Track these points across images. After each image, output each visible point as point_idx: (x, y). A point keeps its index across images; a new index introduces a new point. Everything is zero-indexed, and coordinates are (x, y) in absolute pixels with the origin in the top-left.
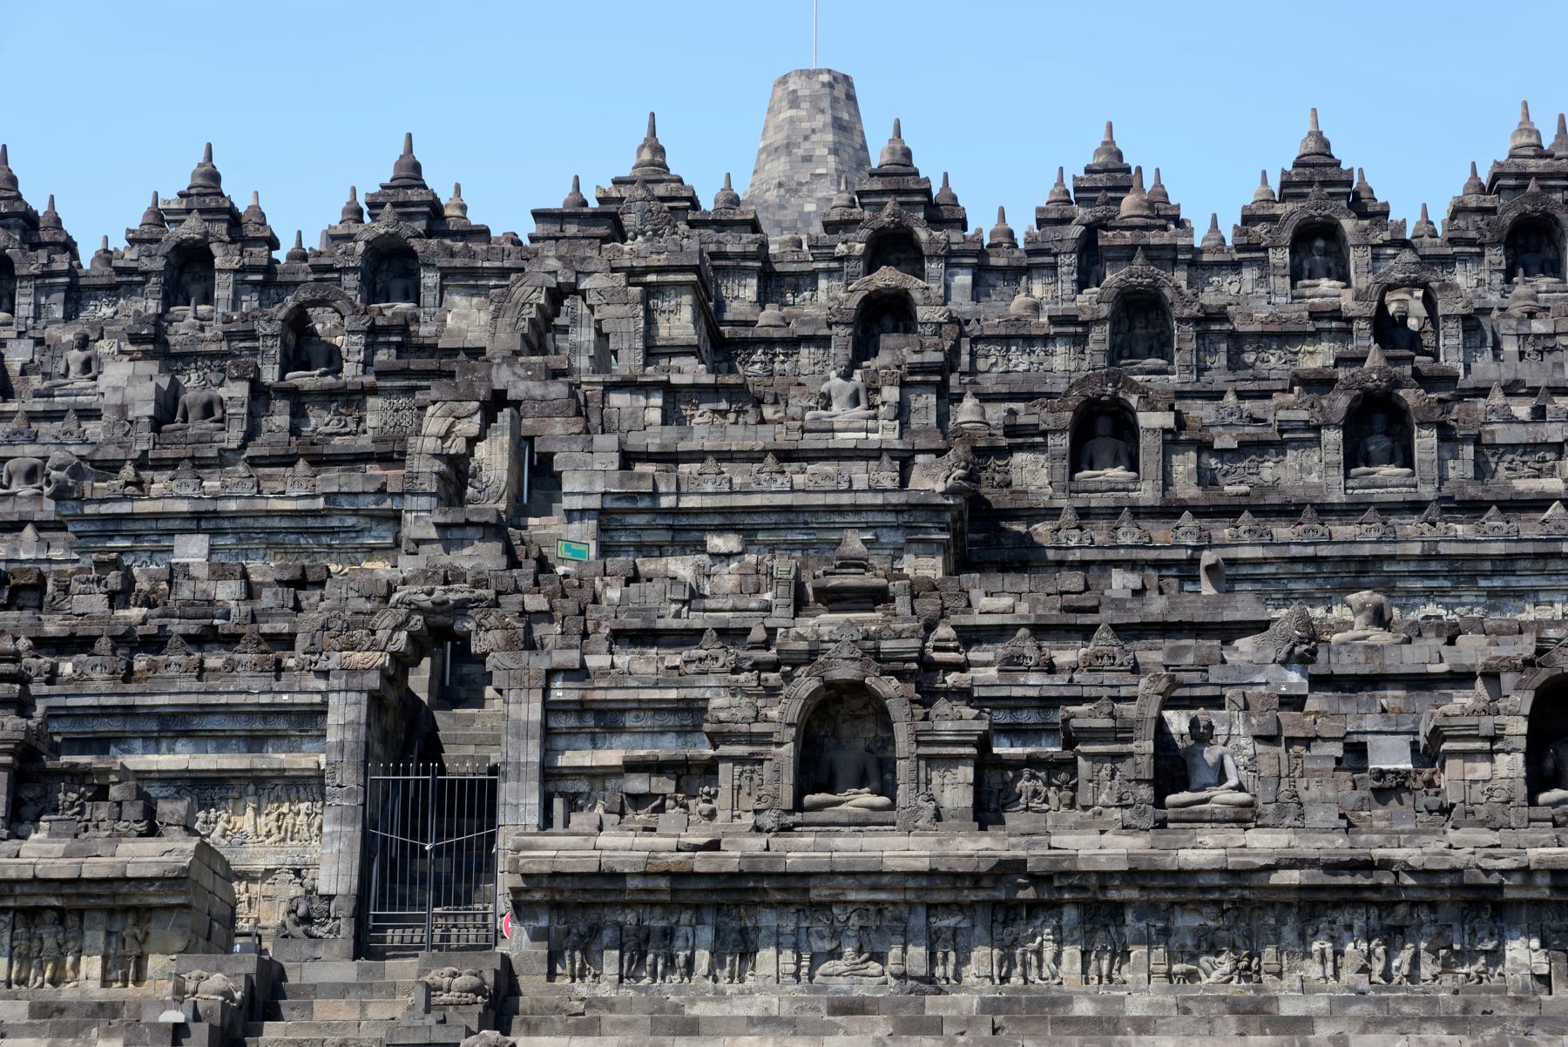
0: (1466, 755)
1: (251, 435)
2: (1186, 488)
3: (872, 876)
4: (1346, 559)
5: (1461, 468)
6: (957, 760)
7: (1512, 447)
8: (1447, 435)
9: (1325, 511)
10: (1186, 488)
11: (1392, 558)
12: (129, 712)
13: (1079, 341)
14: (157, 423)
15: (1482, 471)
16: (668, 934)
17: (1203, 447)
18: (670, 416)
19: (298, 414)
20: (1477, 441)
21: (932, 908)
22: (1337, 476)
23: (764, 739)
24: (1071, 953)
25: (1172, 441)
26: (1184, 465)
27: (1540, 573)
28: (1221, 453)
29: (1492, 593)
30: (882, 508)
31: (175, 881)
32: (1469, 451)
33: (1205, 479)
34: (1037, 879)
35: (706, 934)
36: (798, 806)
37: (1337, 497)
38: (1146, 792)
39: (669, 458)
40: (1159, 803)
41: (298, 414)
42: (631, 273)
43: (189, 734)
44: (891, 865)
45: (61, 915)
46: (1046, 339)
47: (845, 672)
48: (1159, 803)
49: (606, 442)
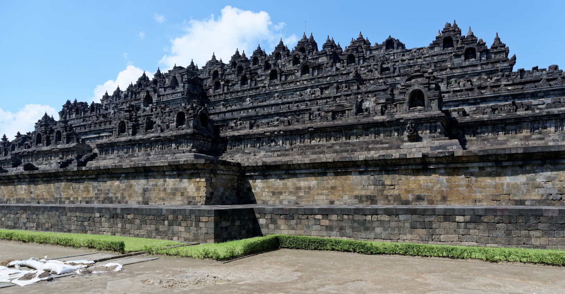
0: (171, 123)
1: (131, 98)
2: (226, 91)
3: (120, 142)
4: (239, 97)
5: (253, 84)
6: (130, 128)
7: (259, 81)
8: (252, 80)
9: (238, 92)
10: (226, 91)
11: (244, 97)
12: (100, 130)
13: (234, 73)
14: (125, 98)
15: (256, 84)
16: (108, 150)
17: (228, 86)
18: (165, 91)
19: (136, 95)
20: (255, 80)
21: (127, 145)
22: (240, 87)
23: (116, 128)
24: (137, 149)
25: (224, 85)
26: (226, 88)
27: (260, 96)
28: (230, 86)
29: (255, 100)
30: (180, 98)
31: (74, 147)
32: (254, 82)
33: (228, 89)
34: (134, 141)
35: (111, 149)
36: (119, 135)
37: (240, 90)
38: (145, 130)
39: (164, 95)
40: (146, 131)
41: (136, 95)
42: (180, 74)
43: (105, 132)
44: (122, 141)
45: (67, 152)
46: (232, 74)
47: (122, 120)
48: (146, 131)
49: (156, 94)
